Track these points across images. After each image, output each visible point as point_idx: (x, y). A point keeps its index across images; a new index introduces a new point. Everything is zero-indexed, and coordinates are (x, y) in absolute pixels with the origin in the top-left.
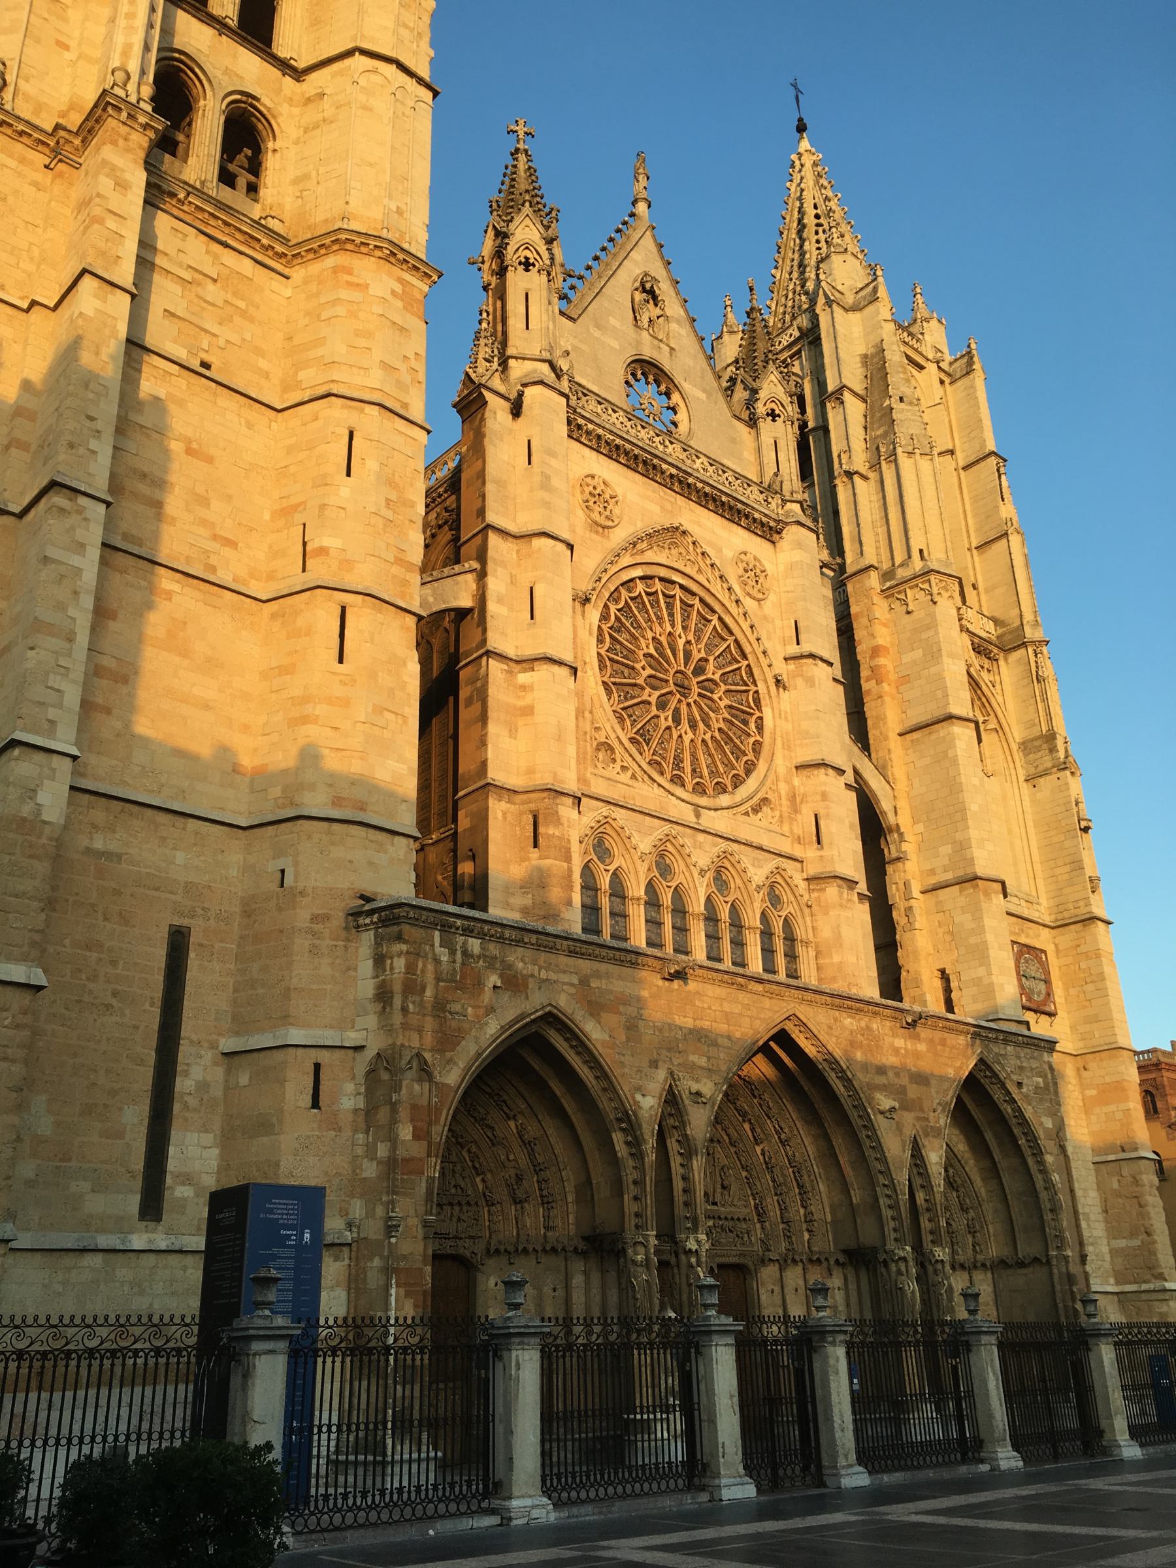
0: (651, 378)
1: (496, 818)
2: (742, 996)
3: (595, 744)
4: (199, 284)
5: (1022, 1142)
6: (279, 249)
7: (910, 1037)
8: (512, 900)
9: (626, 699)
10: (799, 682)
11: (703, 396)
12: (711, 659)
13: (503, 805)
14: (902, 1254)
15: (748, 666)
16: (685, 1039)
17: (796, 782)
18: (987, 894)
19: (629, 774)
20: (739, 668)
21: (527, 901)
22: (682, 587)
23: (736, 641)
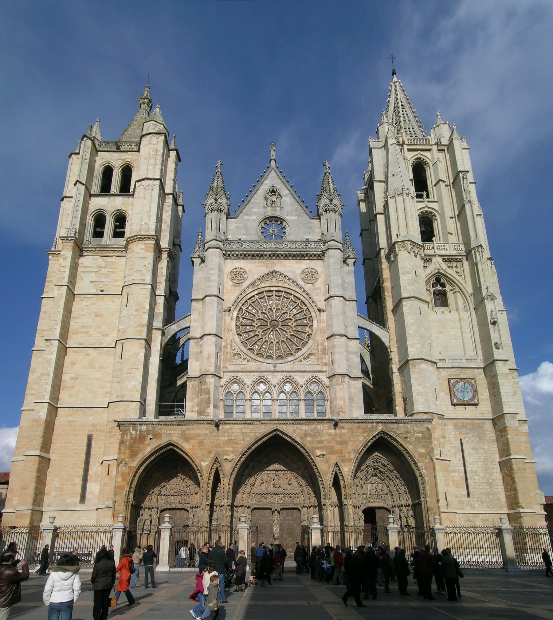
0: (273, 222)
2: (250, 426)
3: (232, 354)
4: (101, 270)
5: (409, 459)
6: (122, 250)
7: (339, 428)
8: (194, 410)
9: (249, 336)
10: (328, 307)
11: (296, 218)
12: (288, 312)
13: (193, 382)
14: (324, 503)
15: (308, 308)
16: (224, 443)
17: (326, 344)
18: (414, 366)
20: (303, 311)
21: (196, 409)
22: (276, 291)
23: (302, 301)
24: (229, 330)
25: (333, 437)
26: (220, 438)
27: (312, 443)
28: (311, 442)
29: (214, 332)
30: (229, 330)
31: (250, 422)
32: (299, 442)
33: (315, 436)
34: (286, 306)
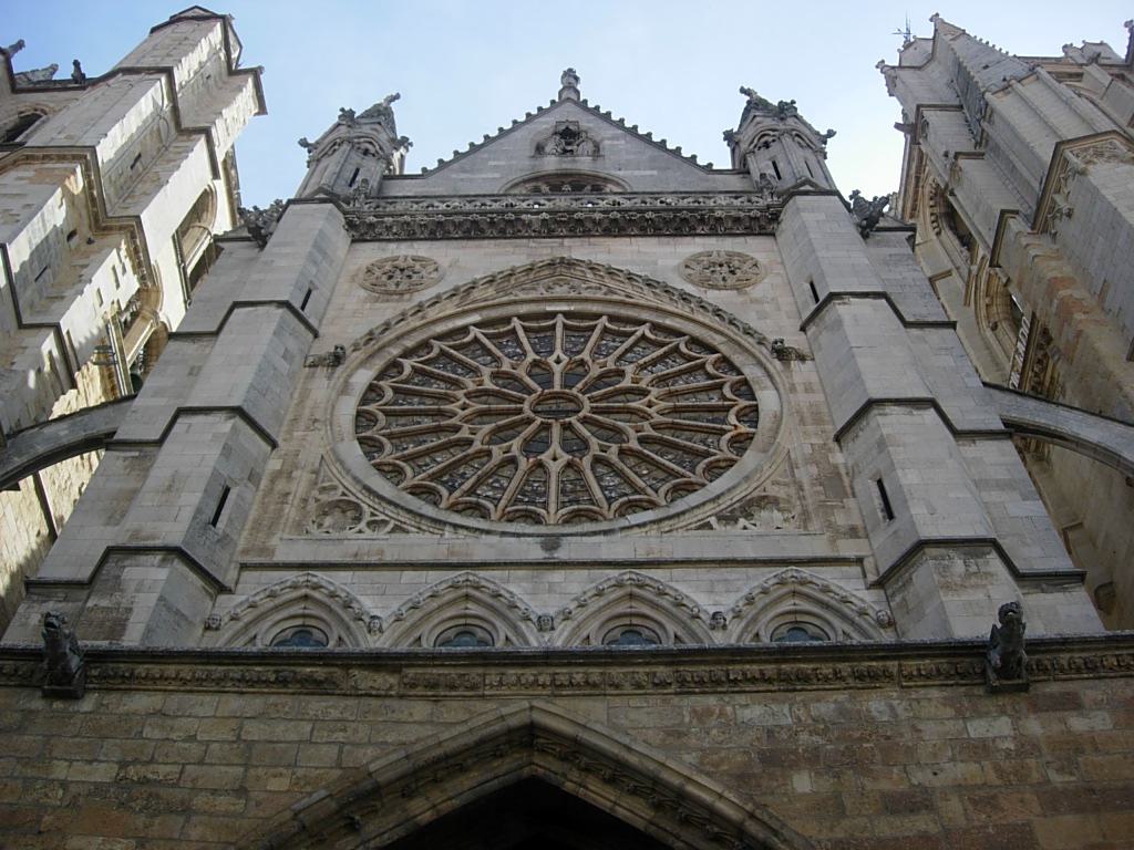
1: (24, 625)
2: (316, 705)
3: (312, 505)
7: (1035, 708)
11: (655, 172)
12: (629, 369)
15: (725, 359)
16: (73, 804)
17: (838, 458)
19: (391, 526)
22: (567, 315)
24: (316, 421)
25: (1006, 765)
26: (60, 771)
27: (841, 812)
28: (831, 807)
29: (234, 403)
30: (316, 421)
31: (320, 672)
32: (721, 806)
33: (859, 764)
34: (618, 352)
